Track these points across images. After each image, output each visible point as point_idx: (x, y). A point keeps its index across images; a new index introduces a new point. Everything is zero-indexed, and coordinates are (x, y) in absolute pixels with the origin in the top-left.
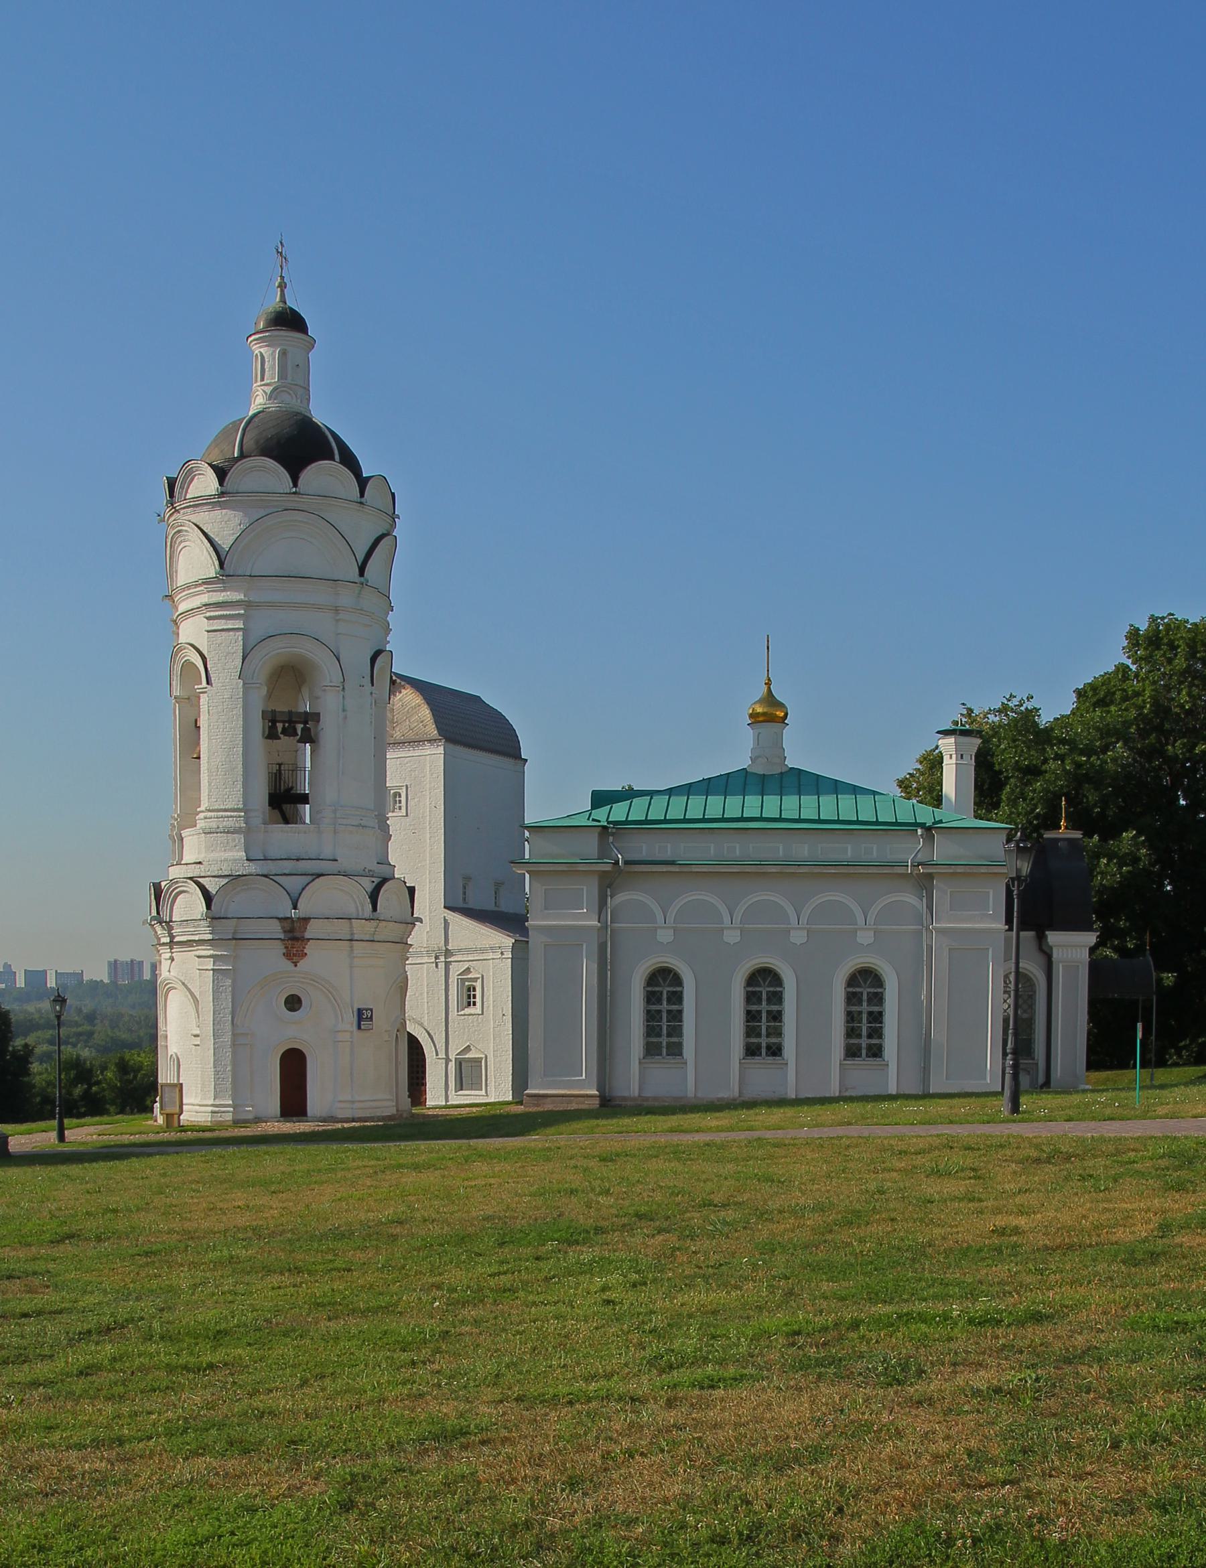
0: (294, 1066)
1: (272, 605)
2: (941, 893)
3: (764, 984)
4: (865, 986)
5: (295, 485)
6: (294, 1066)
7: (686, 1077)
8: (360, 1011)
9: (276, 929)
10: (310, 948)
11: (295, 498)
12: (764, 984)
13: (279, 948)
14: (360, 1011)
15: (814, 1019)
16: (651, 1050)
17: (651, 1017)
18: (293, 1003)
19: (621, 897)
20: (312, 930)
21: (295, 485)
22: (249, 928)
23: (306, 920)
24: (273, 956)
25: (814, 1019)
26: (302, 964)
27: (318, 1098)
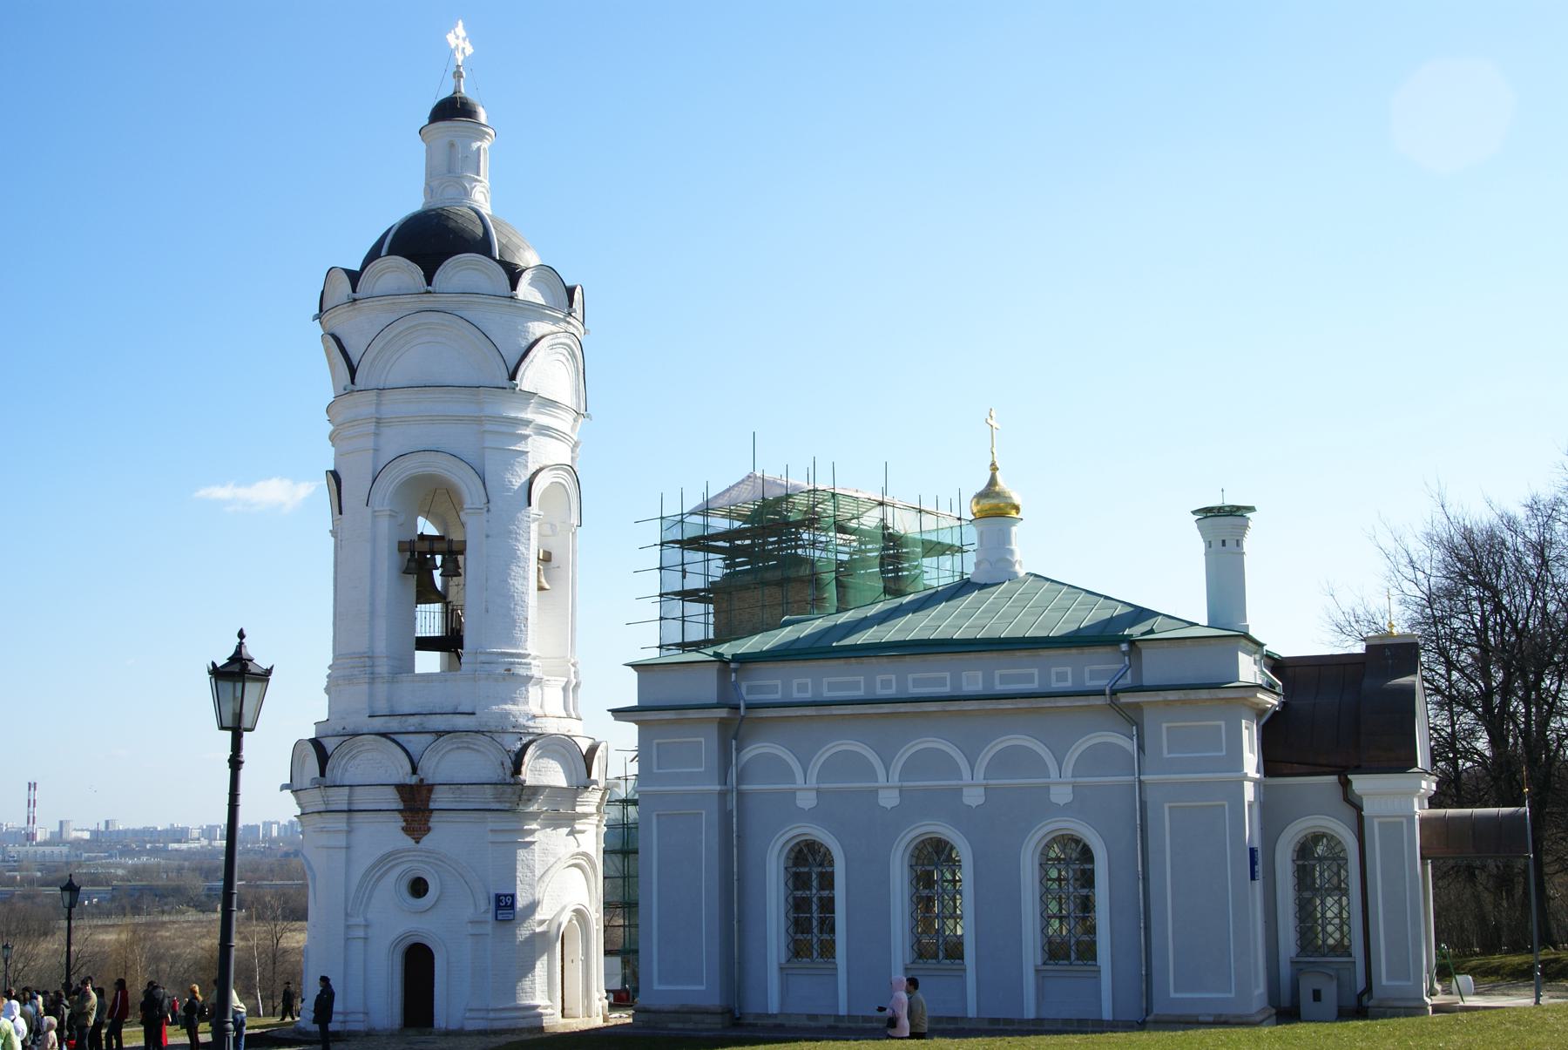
0: (418, 963)
5: (429, 283)
6: (418, 963)
8: (498, 897)
9: (392, 799)
10: (435, 821)
11: (426, 298)
13: (397, 822)
14: (498, 897)
16: (798, 950)
17: (798, 906)
18: (418, 887)
19: (753, 751)
20: (440, 799)
21: (429, 283)
22: (363, 799)
24: (387, 833)
26: (425, 840)
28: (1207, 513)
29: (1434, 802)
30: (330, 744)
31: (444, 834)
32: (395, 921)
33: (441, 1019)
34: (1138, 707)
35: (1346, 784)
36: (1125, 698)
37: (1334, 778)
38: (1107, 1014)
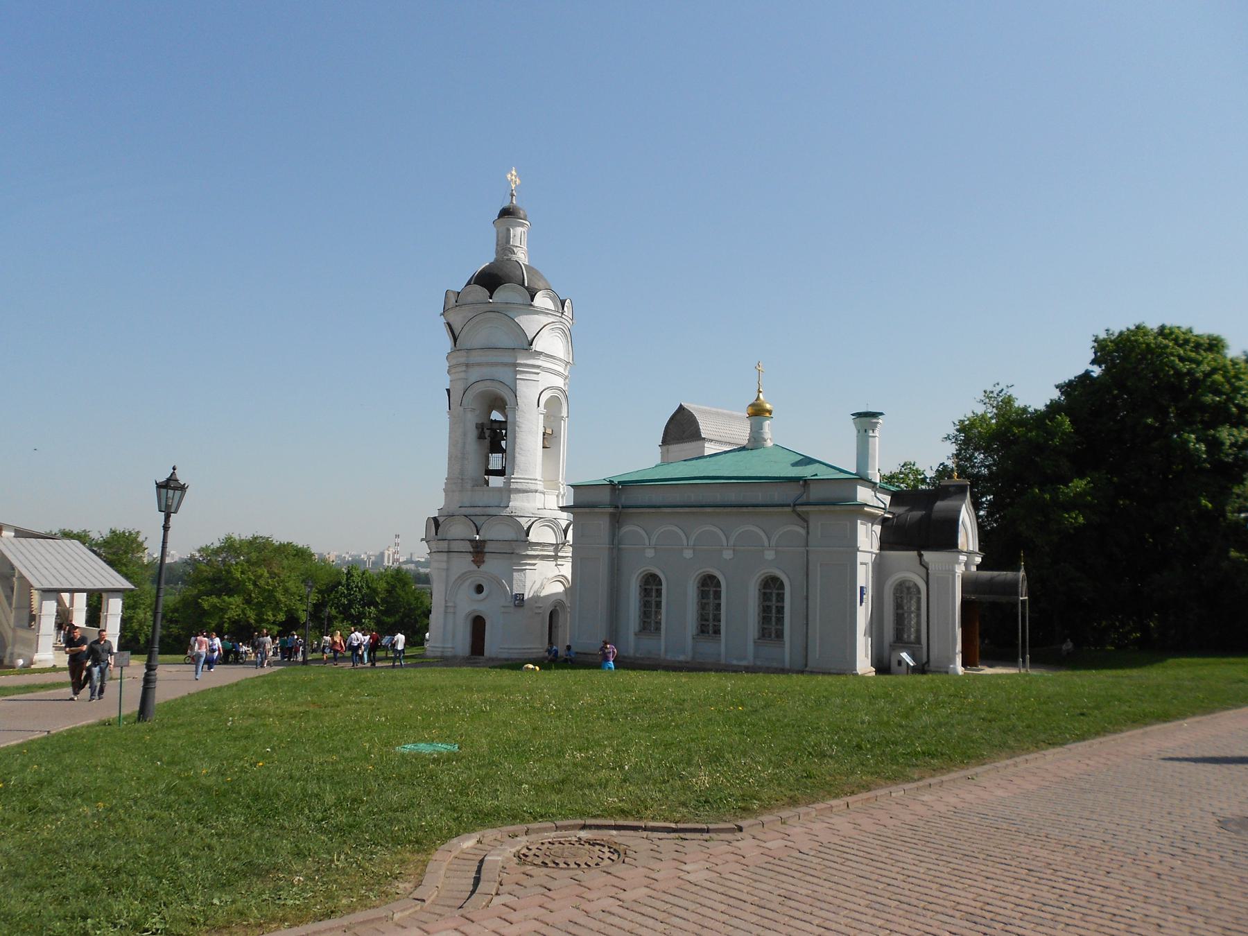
0: (478, 625)
1: (479, 364)
2: (816, 524)
3: (709, 585)
4: (771, 587)
6: (478, 625)
7: (661, 646)
9: (468, 547)
10: (487, 558)
12: (709, 585)
13: (470, 558)
15: (740, 609)
18: (479, 589)
22: (456, 546)
23: (484, 541)
25: (740, 609)
26: (483, 568)
27: (492, 646)
28: (859, 415)
29: (979, 567)
30: (441, 520)
31: (492, 565)
32: (467, 604)
33: (486, 653)
34: (807, 513)
35: (921, 556)
36: (799, 509)
37: (915, 553)
38: (787, 665)
